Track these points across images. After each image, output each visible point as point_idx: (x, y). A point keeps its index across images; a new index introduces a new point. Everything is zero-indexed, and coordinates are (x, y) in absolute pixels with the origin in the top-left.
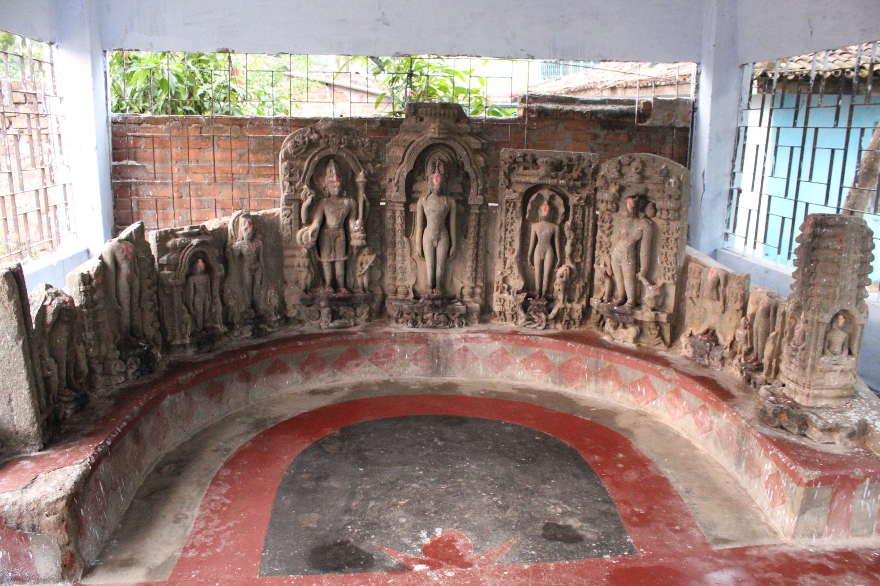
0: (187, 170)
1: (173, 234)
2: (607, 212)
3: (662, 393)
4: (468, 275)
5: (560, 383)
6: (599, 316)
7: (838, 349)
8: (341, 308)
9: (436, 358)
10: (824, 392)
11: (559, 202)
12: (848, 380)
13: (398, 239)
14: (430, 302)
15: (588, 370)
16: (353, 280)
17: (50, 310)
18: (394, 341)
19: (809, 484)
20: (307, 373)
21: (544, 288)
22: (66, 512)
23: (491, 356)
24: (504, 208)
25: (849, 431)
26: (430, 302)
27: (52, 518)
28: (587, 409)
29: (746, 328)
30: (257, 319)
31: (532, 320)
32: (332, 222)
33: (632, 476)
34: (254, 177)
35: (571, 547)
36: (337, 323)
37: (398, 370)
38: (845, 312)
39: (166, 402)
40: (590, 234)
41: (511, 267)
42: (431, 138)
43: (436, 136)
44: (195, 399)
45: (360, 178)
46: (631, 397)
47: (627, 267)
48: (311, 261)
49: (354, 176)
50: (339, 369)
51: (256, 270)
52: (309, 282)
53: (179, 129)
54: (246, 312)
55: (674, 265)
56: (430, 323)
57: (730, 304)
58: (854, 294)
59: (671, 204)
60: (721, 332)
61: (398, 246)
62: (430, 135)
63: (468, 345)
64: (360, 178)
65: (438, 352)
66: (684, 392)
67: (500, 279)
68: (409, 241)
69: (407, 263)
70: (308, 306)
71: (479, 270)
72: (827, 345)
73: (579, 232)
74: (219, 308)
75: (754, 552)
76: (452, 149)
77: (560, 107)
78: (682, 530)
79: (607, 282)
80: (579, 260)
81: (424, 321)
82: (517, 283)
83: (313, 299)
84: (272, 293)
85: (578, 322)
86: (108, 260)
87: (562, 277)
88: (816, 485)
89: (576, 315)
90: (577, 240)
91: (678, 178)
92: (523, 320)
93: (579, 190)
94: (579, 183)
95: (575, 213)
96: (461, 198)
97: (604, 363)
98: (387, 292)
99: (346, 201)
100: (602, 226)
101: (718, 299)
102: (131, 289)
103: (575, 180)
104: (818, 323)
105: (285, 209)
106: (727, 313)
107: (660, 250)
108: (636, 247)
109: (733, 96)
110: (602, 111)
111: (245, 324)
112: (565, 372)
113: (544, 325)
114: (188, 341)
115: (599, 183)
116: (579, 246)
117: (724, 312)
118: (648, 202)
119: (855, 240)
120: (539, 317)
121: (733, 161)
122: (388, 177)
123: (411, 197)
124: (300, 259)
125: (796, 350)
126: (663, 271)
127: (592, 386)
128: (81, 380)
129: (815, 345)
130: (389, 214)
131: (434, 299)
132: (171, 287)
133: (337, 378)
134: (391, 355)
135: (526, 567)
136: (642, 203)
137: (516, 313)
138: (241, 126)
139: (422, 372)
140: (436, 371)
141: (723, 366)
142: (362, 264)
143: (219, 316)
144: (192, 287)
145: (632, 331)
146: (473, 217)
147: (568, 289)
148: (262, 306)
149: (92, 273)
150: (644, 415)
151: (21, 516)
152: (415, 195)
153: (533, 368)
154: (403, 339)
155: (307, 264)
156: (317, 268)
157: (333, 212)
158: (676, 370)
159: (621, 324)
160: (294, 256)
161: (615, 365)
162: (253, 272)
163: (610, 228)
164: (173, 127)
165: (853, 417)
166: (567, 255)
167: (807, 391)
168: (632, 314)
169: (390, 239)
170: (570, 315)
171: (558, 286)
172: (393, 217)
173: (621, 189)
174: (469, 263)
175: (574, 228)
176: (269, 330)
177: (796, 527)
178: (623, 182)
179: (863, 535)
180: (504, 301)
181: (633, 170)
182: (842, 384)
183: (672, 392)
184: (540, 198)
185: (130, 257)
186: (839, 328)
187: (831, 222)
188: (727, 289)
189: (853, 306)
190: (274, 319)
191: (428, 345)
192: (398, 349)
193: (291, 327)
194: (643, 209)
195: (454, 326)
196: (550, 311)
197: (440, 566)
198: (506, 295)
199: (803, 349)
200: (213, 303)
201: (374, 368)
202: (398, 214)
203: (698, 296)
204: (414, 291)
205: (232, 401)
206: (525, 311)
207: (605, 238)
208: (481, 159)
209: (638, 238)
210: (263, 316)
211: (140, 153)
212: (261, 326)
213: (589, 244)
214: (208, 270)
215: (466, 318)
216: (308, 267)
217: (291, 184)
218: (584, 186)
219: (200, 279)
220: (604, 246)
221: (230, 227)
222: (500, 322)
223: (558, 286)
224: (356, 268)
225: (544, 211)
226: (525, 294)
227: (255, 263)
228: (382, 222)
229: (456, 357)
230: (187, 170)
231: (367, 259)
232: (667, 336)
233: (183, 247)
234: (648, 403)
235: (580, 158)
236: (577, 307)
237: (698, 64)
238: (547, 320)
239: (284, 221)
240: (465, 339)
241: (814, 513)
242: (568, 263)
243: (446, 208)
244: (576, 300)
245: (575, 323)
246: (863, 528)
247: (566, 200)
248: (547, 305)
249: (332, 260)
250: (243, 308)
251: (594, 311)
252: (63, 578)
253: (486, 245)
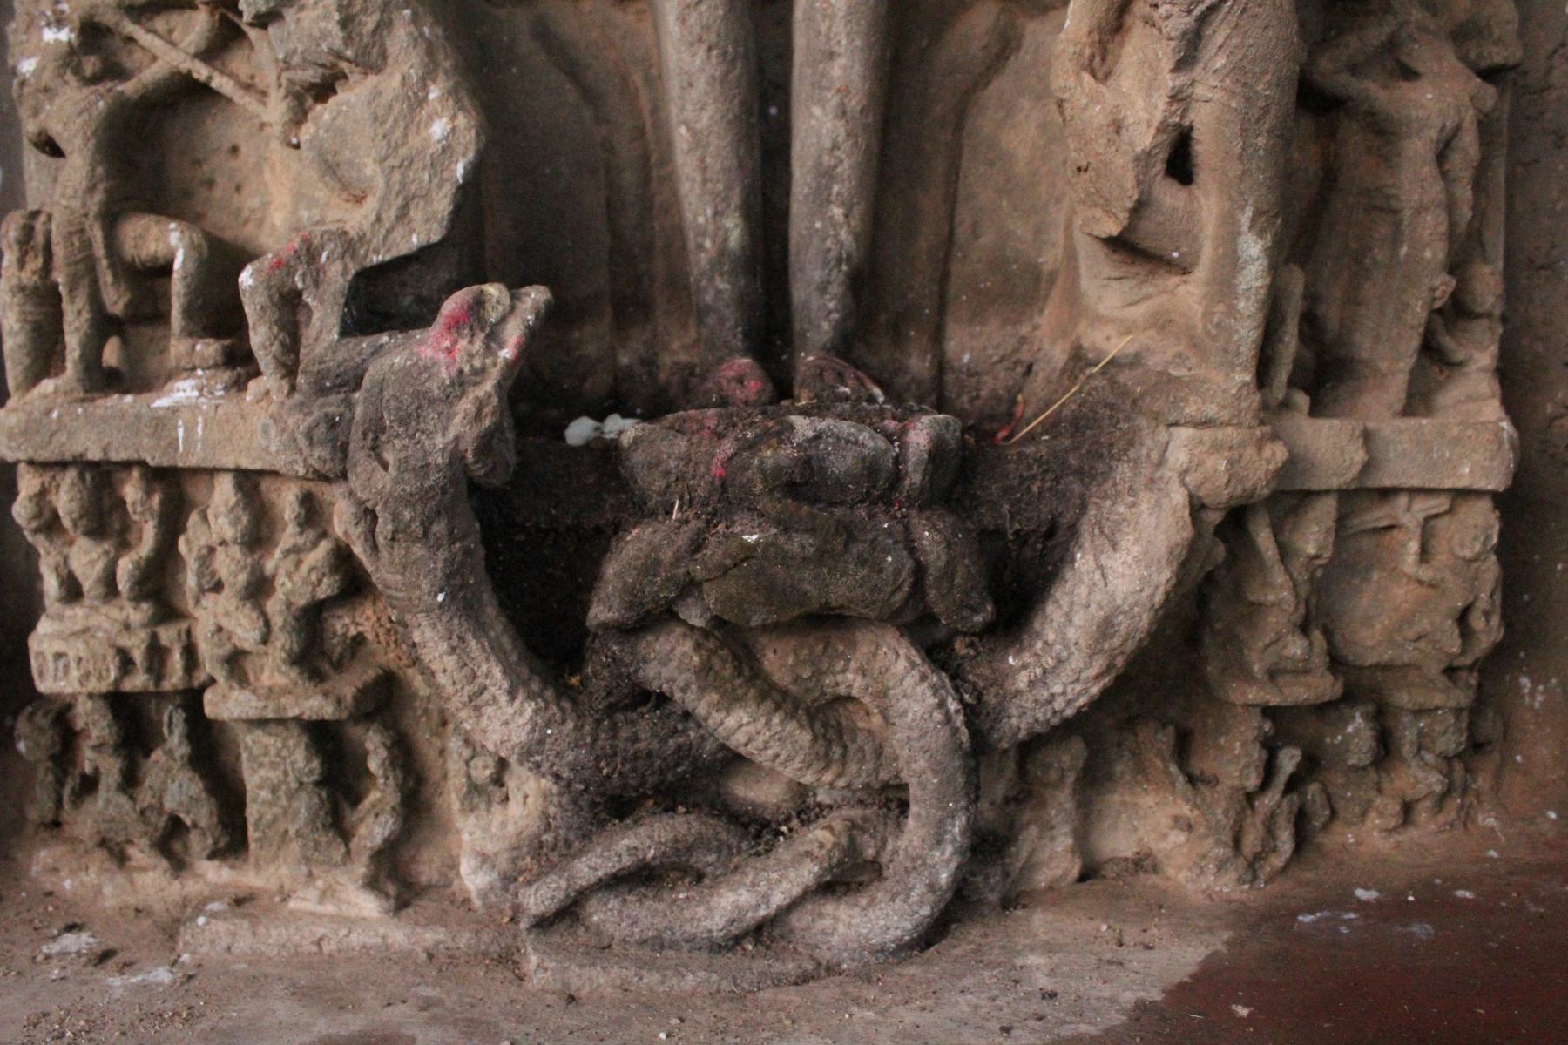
21: (824, 228)
31: (697, 781)
92: (528, 800)
113: (926, 851)
120: (828, 719)
137: (386, 699)
196: (1016, 585)
222: (152, 882)
226: (517, 311)
248: (958, 477)
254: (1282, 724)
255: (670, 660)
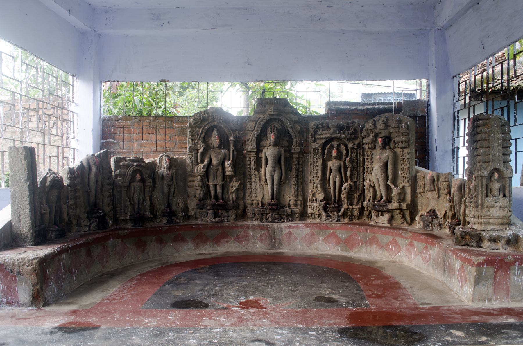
0: (141, 145)
1: (124, 159)
2: (370, 150)
3: (403, 246)
4: (293, 193)
5: (346, 251)
6: (368, 211)
7: (496, 193)
8: (220, 211)
9: (273, 238)
10: (491, 220)
11: (343, 147)
12: (505, 212)
13: (252, 173)
14: (270, 207)
15: (361, 240)
16: (227, 196)
17: (49, 179)
18: (249, 229)
19: (479, 265)
20: (197, 244)
21: (337, 199)
22: (37, 265)
23: (305, 236)
24: (312, 154)
25: (506, 239)
26: (270, 207)
27: (29, 268)
28: (359, 261)
29: (450, 202)
30: (171, 214)
31: (330, 216)
32: (215, 162)
33: (379, 282)
34: (178, 149)
35: (329, 304)
36: (217, 219)
37: (251, 245)
38: (497, 170)
39: (110, 242)
40: (361, 165)
41: (317, 187)
42: (270, 115)
43: (272, 113)
44: (128, 246)
45: (231, 138)
46: (386, 253)
47: (381, 178)
48: (203, 184)
49: (228, 137)
50: (216, 244)
51: (171, 185)
52: (201, 195)
53: (138, 123)
54: (164, 209)
55: (408, 175)
56: (270, 219)
57: (441, 192)
58: (501, 158)
59: (403, 138)
60: (438, 210)
61: (253, 177)
62: (269, 113)
63: (291, 230)
64: (231, 138)
65: (274, 235)
66: (415, 242)
67: (311, 194)
68: (259, 174)
69: (258, 186)
70: (201, 209)
71: (299, 190)
72: (489, 192)
73: (354, 164)
74: (148, 203)
75: (446, 308)
76: (282, 122)
77: (349, 107)
78: (402, 300)
79: (371, 190)
80: (355, 180)
81: (267, 219)
82: (320, 196)
83: (204, 205)
84: (180, 200)
85: (357, 218)
86: (85, 164)
87: (345, 189)
88: (483, 266)
89: (355, 213)
90: (354, 168)
91: (407, 123)
93: (354, 141)
94: (353, 136)
95: (352, 153)
96: (287, 149)
97: (370, 235)
98: (247, 205)
99: (223, 151)
100: (367, 159)
101: (435, 190)
102: (97, 181)
103: (351, 135)
104: (482, 177)
105: (189, 155)
106: (440, 197)
107: (400, 166)
108: (386, 165)
109: (449, 95)
110: (373, 109)
111: (164, 216)
112: (348, 243)
113: (336, 219)
114: (128, 218)
115: (364, 133)
116: (355, 172)
117: (438, 197)
118: (391, 140)
119: (497, 126)
120: (334, 214)
121: (453, 132)
122: (247, 138)
123: (259, 150)
124: (197, 182)
125: (472, 198)
126: (402, 179)
127: (364, 250)
128: (63, 224)
129: (482, 191)
130: (248, 159)
131: (272, 205)
132: (120, 187)
133: (214, 249)
134: (247, 236)
135: (299, 310)
136: (387, 141)
137: (320, 214)
138: (172, 121)
139: (265, 247)
140: (273, 247)
141: (441, 229)
142: (232, 187)
143: (148, 208)
144: (133, 189)
145: (387, 216)
146: (294, 159)
147: (350, 197)
148: (174, 208)
149: (75, 168)
150: (395, 262)
151: (13, 265)
152: (261, 148)
153: (330, 243)
154: (254, 228)
155: (200, 185)
156: (207, 189)
157: (215, 156)
158: (410, 232)
159: (380, 213)
160: (194, 181)
161: (376, 235)
162: (169, 186)
163: (371, 159)
164: (135, 122)
165: (509, 232)
166: (348, 178)
167: (480, 220)
168: (386, 206)
169: (248, 173)
170: (352, 212)
171: (343, 196)
172: (250, 161)
173: (376, 136)
174: (293, 186)
175: (351, 161)
176: (178, 221)
177: (473, 294)
178: (377, 131)
179: (519, 301)
180: (314, 207)
181: (381, 122)
182: (502, 215)
183: (408, 245)
184: (332, 147)
185: (97, 164)
186: (495, 180)
187: (481, 117)
188: (439, 183)
189: (502, 166)
190: (180, 215)
191: (269, 231)
192: (251, 233)
193: (191, 221)
194: (388, 144)
195: (284, 222)
196: (339, 211)
197: (247, 308)
198: (315, 204)
199: (475, 196)
200: (144, 199)
201: (237, 244)
202: (252, 158)
203: (424, 192)
204: (262, 203)
205: (151, 253)
206: (326, 212)
207: (369, 166)
208: (298, 126)
209: (386, 160)
210: (174, 212)
211: (117, 136)
212: (173, 218)
213: (361, 171)
214: (143, 180)
215: (291, 217)
216: (201, 187)
217: (193, 140)
218: (356, 138)
219: (137, 185)
220: (369, 170)
221: (158, 162)
223: (343, 196)
224: (229, 189)
225: (334, 153)
226: (325, 202)
227: (170, 181)
228: (244, 165)
229: (285, 238)
230: (141, 145)
231: (235, 184)
232: (408, 218)
233: (129, 166)
234: (396, 254)
235: (352, 123)
236: (356, 208)
237: (428, 80)
238: (338, 216)
239: (188, 161)
240: (290, 227)
241: (484, 285)
242: (349, 182)
243: (278, 152)
244: (355, 204)
245: (355, 218)
246: (518, 296)
247: (346, 146)
248: (338, 207)
249: (215, 183)
250: (163, 208)
251: (366, 209)
252: (32, 305)
253: (303, 177)
254: (350, 216)
255: (329, 212)
